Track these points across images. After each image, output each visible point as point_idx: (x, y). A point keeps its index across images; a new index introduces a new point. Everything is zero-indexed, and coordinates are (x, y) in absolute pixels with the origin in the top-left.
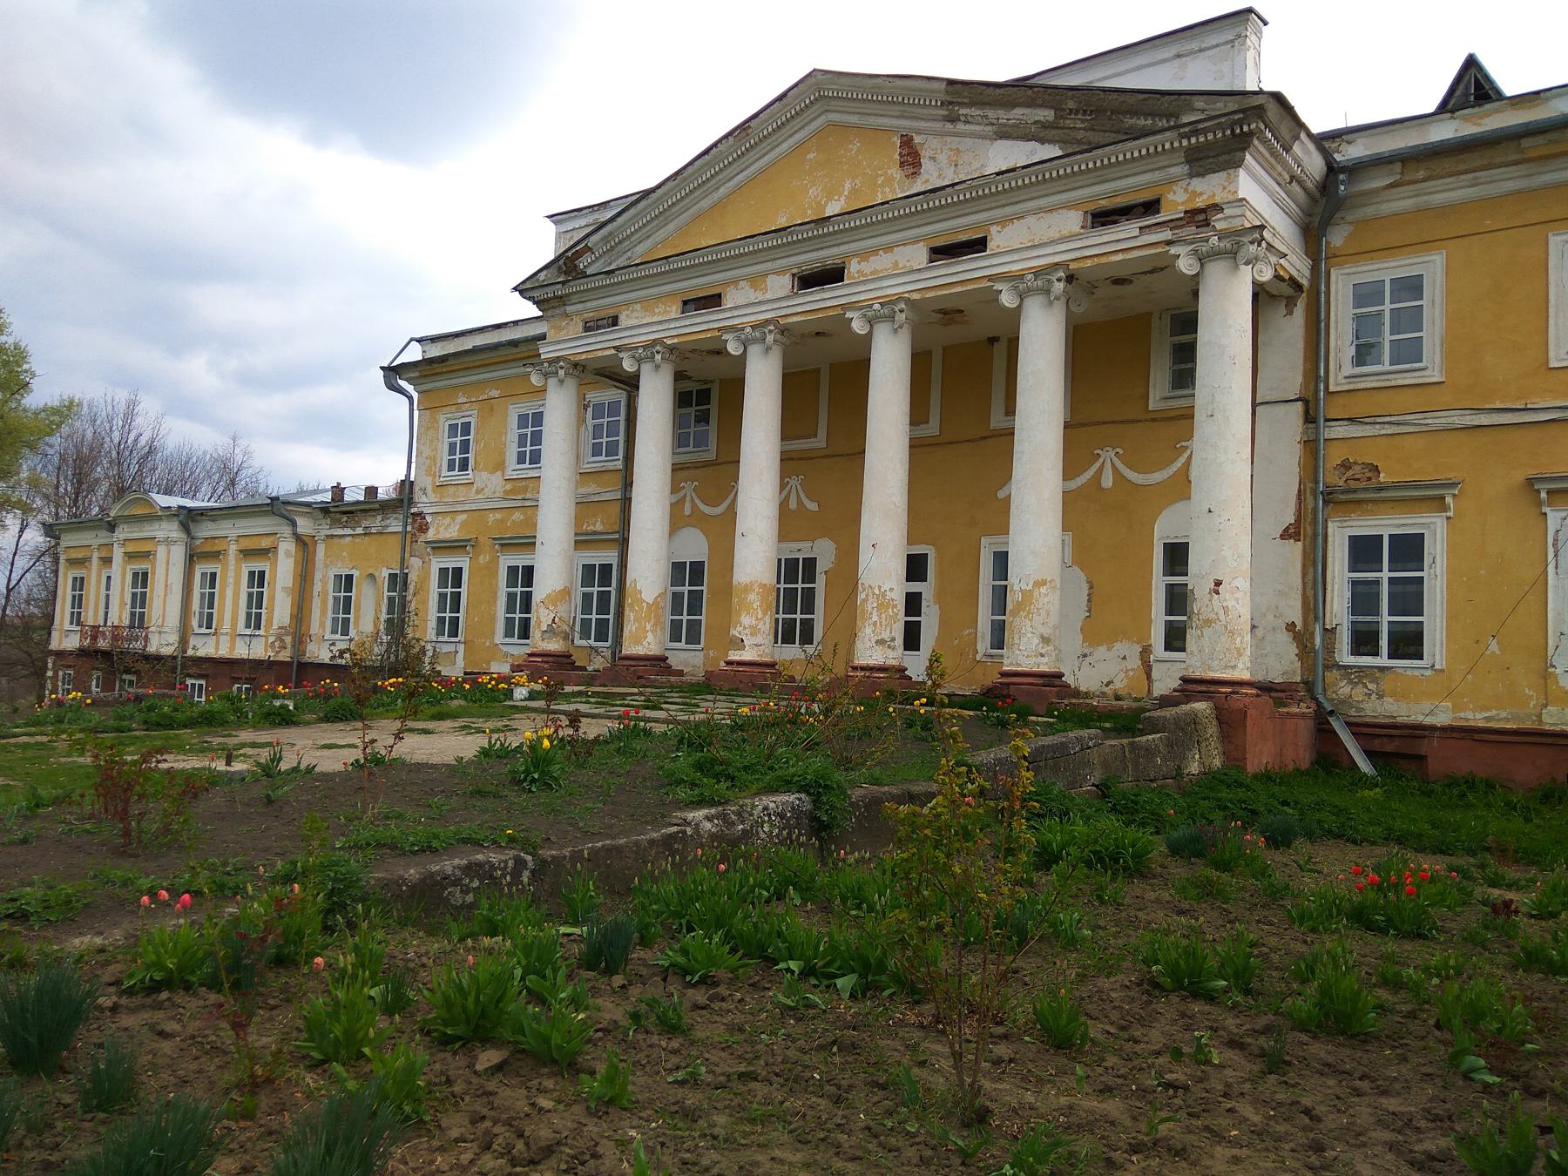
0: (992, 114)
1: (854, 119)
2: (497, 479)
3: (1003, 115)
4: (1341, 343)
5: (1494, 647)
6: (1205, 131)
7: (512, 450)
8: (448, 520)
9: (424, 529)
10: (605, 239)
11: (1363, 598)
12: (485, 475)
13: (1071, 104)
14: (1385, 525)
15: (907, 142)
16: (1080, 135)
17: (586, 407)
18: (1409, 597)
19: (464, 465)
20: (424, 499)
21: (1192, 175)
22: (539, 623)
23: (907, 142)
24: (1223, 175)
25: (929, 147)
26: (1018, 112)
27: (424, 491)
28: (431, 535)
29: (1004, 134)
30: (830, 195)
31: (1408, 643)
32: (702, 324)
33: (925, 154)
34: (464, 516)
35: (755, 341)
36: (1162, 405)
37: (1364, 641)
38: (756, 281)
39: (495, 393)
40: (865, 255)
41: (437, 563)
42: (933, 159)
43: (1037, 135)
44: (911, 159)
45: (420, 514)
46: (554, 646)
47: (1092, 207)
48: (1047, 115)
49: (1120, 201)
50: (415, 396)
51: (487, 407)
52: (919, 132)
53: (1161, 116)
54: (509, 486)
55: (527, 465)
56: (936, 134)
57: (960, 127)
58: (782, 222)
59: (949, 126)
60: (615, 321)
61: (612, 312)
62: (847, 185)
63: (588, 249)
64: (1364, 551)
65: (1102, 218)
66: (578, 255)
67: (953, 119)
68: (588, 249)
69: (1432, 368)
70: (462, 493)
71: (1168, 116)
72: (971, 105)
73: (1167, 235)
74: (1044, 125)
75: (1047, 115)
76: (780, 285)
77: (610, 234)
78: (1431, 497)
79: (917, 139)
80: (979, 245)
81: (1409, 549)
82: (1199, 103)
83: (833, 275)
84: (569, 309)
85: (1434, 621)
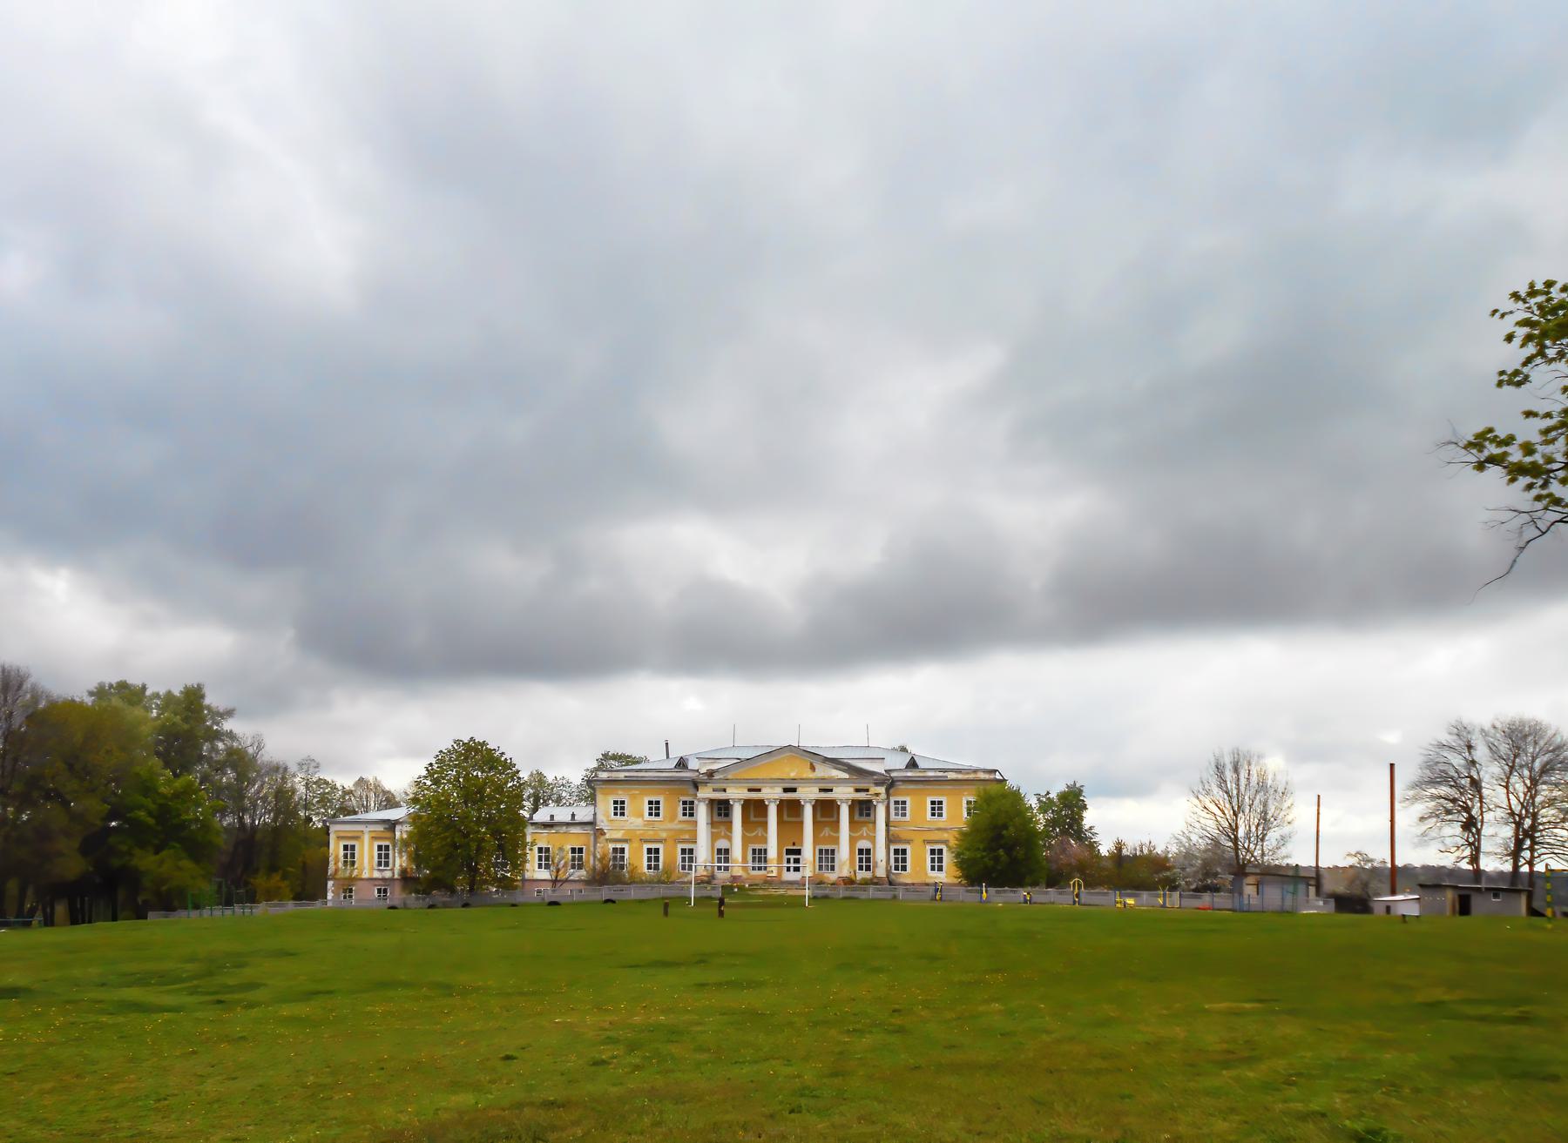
2: (639, 821)
4: (892, 811)
7: (647, 811)
11: (896, 860)
14: (900, 847)
18: (904, 860)
25: (818, 766)
31: (904, 868)
32: (754, 795)
37: (897, 868)
44: (813, 768)
51: (633, 797)
64: (896, 852)
65: (857, 790)
69: (908, 818)
76: (780, 790)
78: (908, 842)
81: (904, 852)
83: (794, 790)
85: (908, 864)
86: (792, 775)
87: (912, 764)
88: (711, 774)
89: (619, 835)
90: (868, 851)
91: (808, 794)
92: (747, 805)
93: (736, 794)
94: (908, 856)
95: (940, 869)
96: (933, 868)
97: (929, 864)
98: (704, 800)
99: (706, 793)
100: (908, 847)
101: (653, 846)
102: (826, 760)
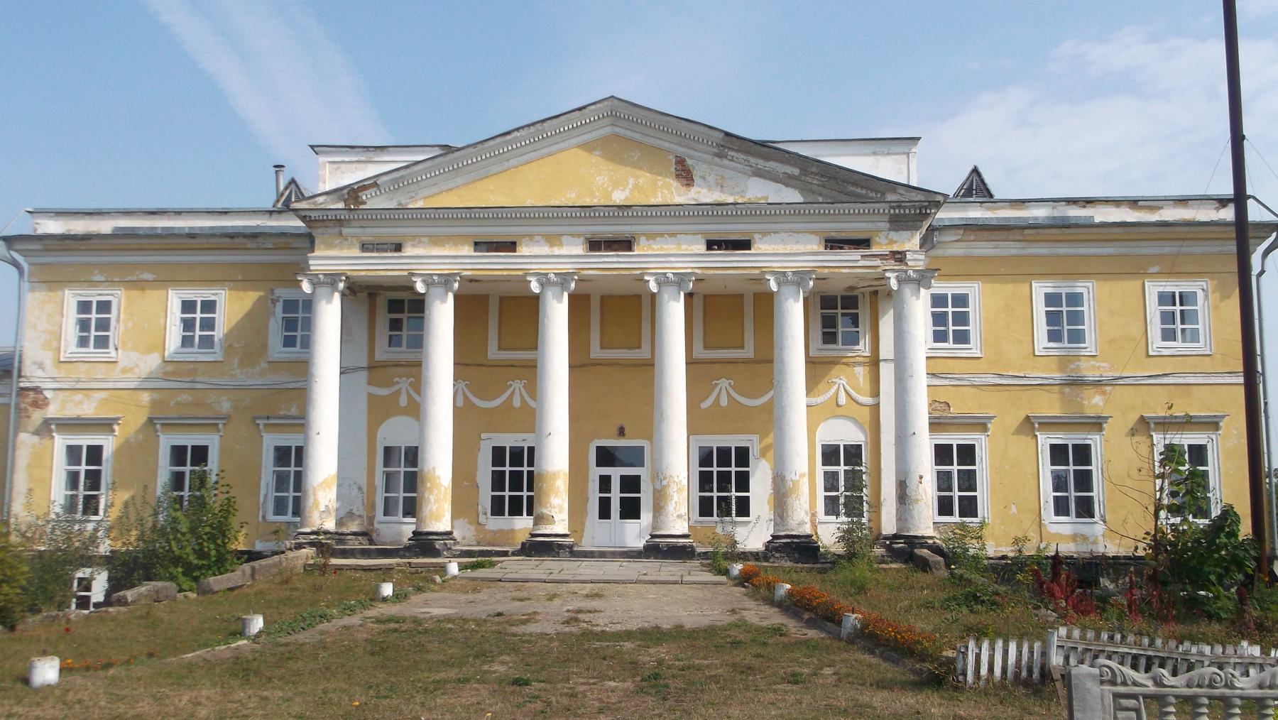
0: (753, 160)
1: (638, 136)
3: (761, 163)
5: (1014, 509)
6: (905, 208)
8: (78, 397)
9: (40, 403)
10: (395, 181)
12: (134, 355)
13: (814, 169)
15: (680, 162)
16: (815, 188)
17: (274, 302)
18: (968, 481)
19: (102, 342)
20: (39, 373)
21: (890, 230)
22: (316, 504)
23: (680, 162)
24: (909, 233)
25: (698, 170)
26: (772, 165)
27: (41, 366)
28: (52, 411)
29: (759, 173)
30: (617, 184)
32: (495, 264)
33: (696, 175)
34: (103, 395)
35: (555, 284)
36: (818, 354)
38: (552, 240)
39: (148, 276)
40: (652, 236)
41: (60, 442)
42: (703, 178)
43: (787, 181)
45: (37, 390)
46: (330, 525)
47: (826, 235)
48: (796, 172)
49: (844, 236)
50: (25, 266)
52: (691, 157)
53: (872, 190)
54: (170, 368)
55: (196, 349)
56: (705, 162)
57: (725, 162)
58: (570, 197)
59: (716, 159)
60: (398, 248)
61: (396, 240)
62: (631, 181)
63: (375, 185)
65: (833, 244)
66: (364, 188)
67: (720, 156)
68: (375, 185)
69: (974, 348)
70: (99, 372)
71: (877, 192)
72: (738, 151)
73: (878, 262)
74: (790, 176)
75: (796, 172)
77: (402, 177)
79: (689, 162)
80: (745, 245)
82: (901, 190)
83: (625, 244)
84: (345, 231)
86: (619, 197)
87: (976, 187)
88: (352, 194)
89: (88, 408)
90: (853, 453)
91: (670, 258)
92: (473, 305)
93: (432, 261)
94: (983, 468)
95: (1085, 508)
96: (1061, 507)
97: (1048, 493)
98: (332, 279)
99: (335, 258)
100: (980, 441)
101: (190, 440)
102: (731, 144)
